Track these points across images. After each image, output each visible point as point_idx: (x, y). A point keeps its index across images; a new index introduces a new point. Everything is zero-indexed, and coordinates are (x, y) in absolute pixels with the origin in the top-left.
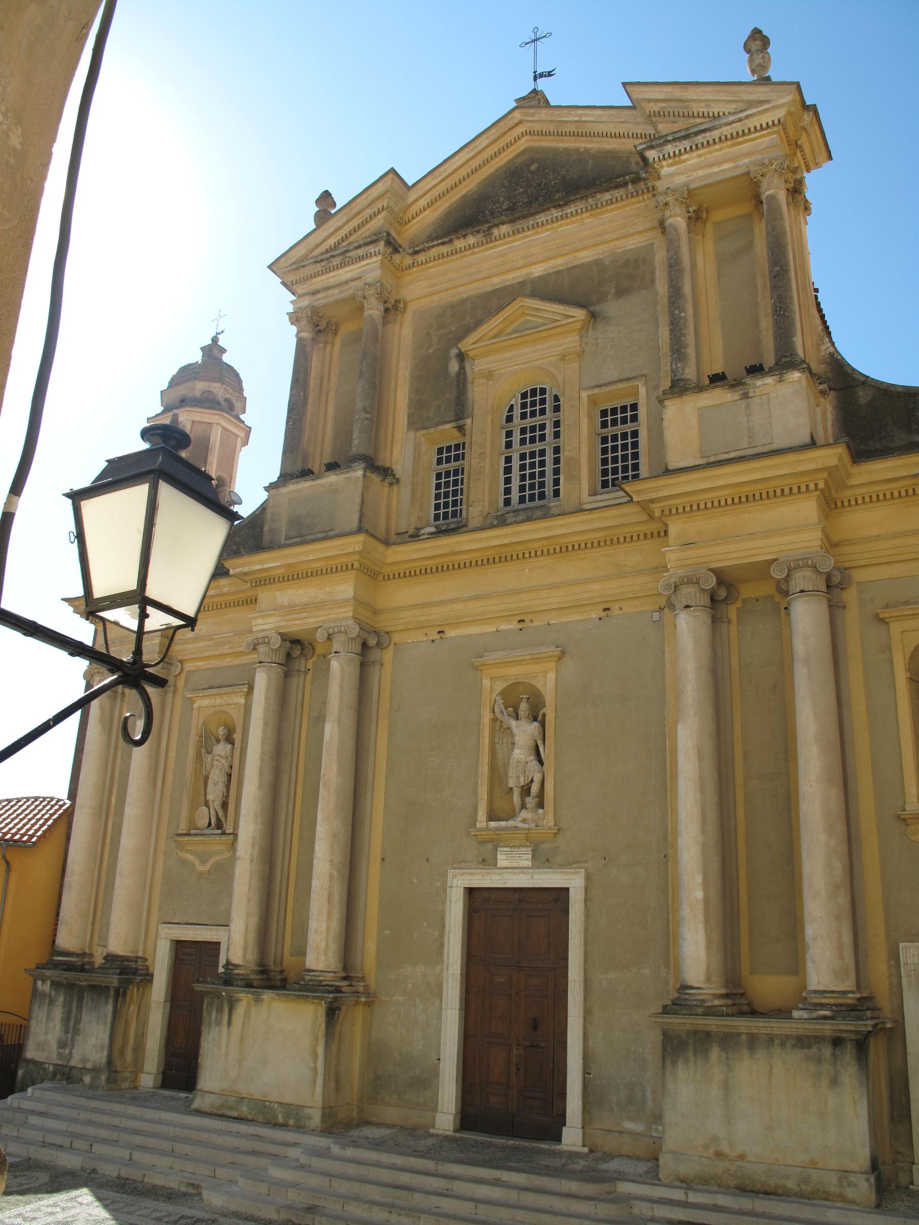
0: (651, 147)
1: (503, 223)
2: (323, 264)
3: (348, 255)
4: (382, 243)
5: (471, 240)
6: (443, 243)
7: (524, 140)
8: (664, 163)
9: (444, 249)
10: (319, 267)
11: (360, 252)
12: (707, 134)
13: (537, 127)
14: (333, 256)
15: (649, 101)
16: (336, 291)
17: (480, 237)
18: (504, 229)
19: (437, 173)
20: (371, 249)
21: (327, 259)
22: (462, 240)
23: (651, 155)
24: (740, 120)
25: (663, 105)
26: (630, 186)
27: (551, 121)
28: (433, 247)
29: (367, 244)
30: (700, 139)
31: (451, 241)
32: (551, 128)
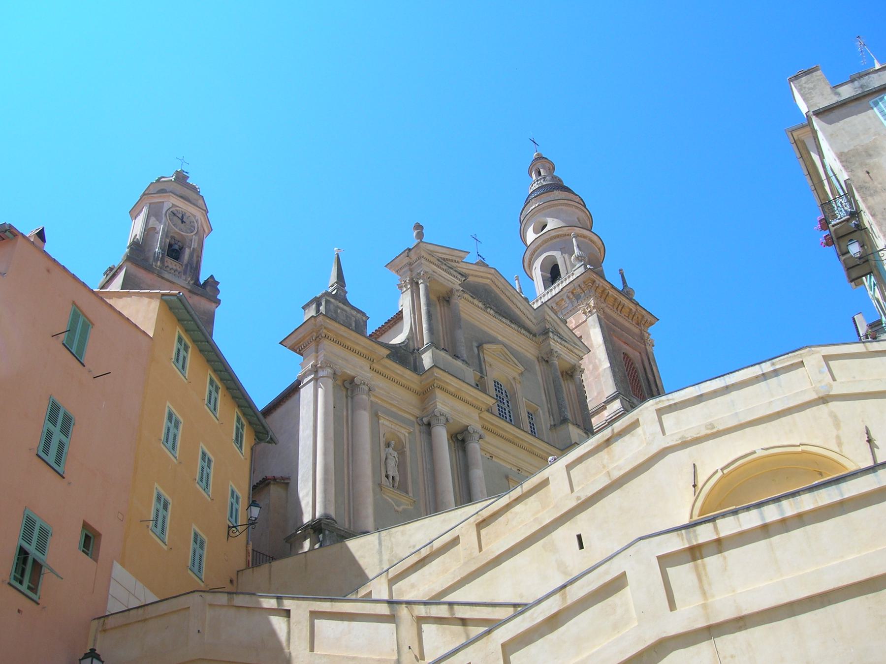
0: (553, 333)
1: (493, 310)
2: (439, 263)
3: (450, 269)
4: (464, 279)
5: (480, 305)
6: (471, 296)
7: (489, 280)
8: (552, 341)
9: (471, 299)
10: (437, 262)
11: (455, 273)
12: (565, 343)
13: (496, 281)
14: (445, 264)
15: (548, 315)
16: (443, 279)
17: (483, 307)
18: (492, 312)
19: (468, 264)
20: (459, 276)
21: (443, 263)
22: (477, 301)
23: (551, 335)
24: (574, 347)
25: (552, 320)
26: (531, 335)
27: (503, 285)
28: (468, 294)
29: (460, 273)
30: (563, 342)
31: (474, 298)
32: (501, 287)
